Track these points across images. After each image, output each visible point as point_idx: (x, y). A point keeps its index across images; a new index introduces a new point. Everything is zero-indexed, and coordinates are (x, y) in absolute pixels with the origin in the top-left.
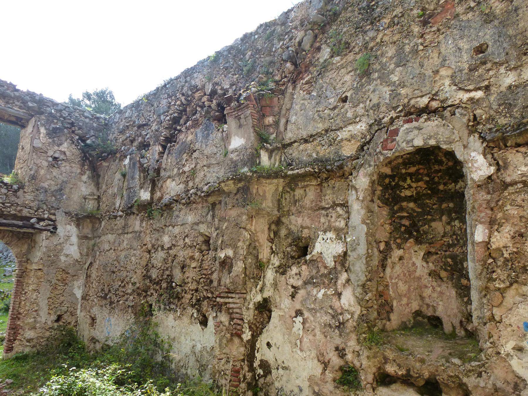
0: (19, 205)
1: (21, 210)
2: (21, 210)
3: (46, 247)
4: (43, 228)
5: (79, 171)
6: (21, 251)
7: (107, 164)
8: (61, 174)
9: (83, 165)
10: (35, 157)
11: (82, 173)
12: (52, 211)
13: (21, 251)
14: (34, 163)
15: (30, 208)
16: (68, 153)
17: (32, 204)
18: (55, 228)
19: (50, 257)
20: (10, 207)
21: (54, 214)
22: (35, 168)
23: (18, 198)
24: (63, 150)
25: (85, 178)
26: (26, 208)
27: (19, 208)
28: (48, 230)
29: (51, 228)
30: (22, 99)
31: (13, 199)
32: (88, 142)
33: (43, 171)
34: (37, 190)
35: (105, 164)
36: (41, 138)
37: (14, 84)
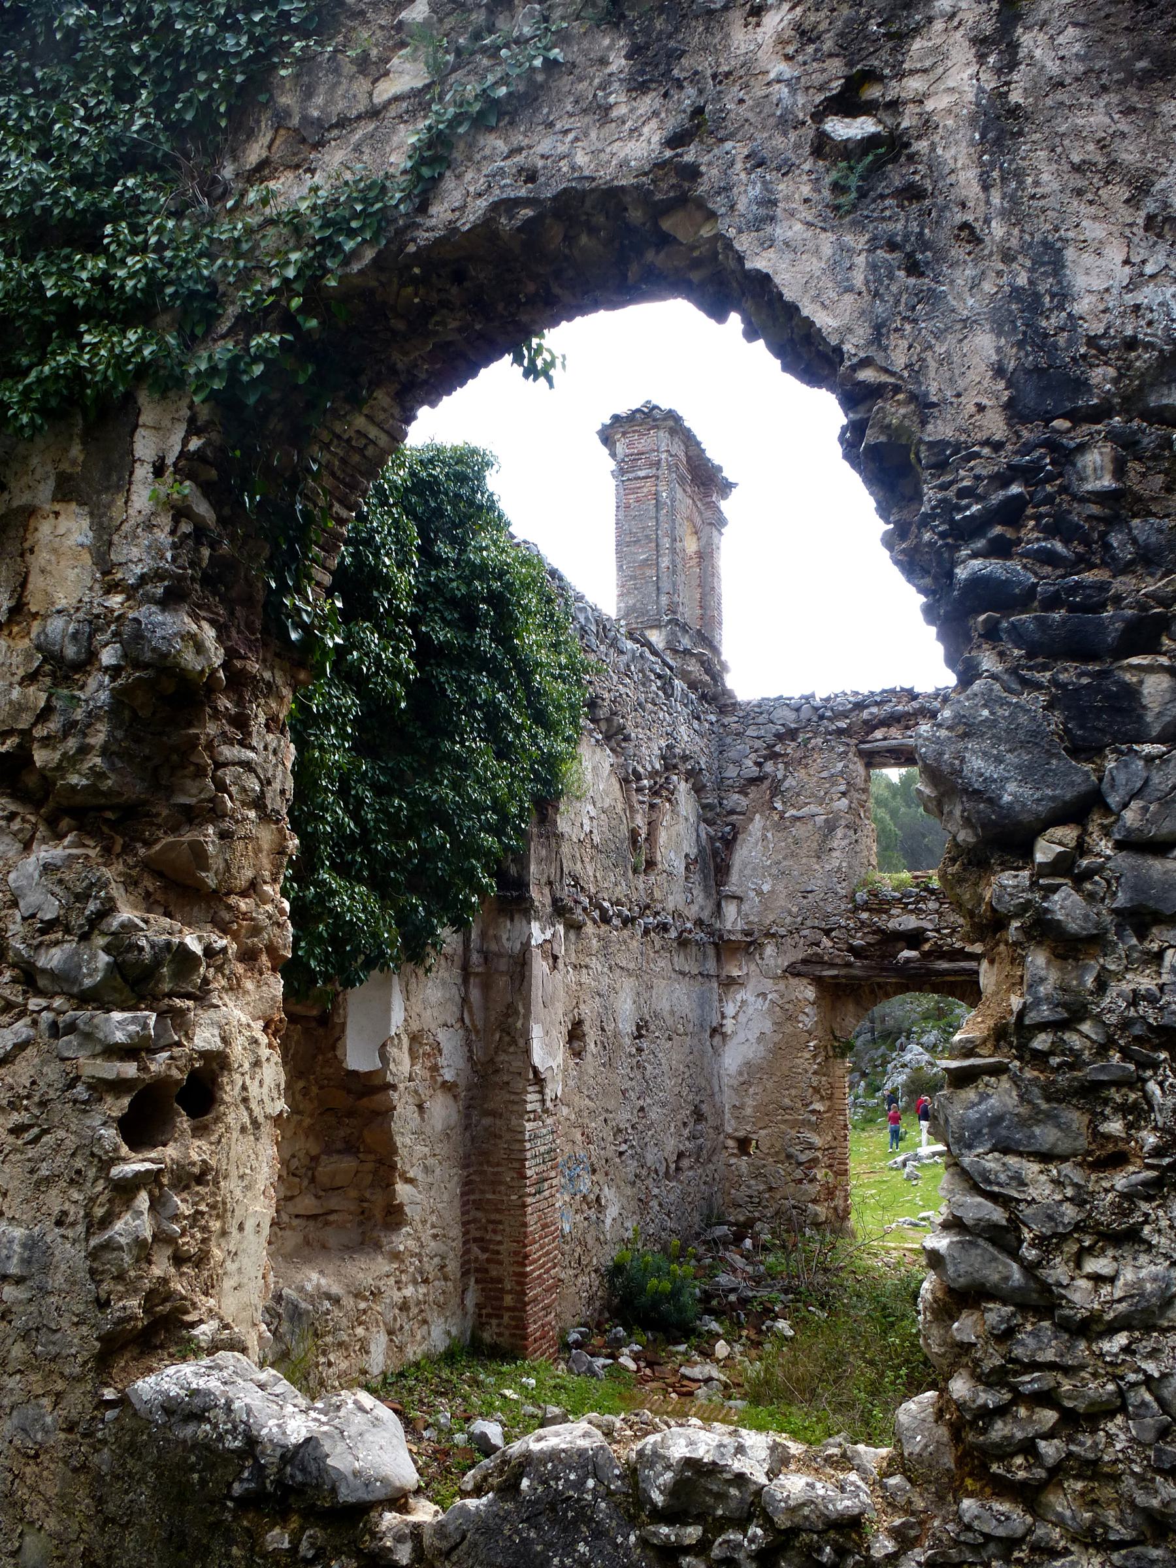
20: (951, 935)
30: (929, 711)
37: (907, 686)
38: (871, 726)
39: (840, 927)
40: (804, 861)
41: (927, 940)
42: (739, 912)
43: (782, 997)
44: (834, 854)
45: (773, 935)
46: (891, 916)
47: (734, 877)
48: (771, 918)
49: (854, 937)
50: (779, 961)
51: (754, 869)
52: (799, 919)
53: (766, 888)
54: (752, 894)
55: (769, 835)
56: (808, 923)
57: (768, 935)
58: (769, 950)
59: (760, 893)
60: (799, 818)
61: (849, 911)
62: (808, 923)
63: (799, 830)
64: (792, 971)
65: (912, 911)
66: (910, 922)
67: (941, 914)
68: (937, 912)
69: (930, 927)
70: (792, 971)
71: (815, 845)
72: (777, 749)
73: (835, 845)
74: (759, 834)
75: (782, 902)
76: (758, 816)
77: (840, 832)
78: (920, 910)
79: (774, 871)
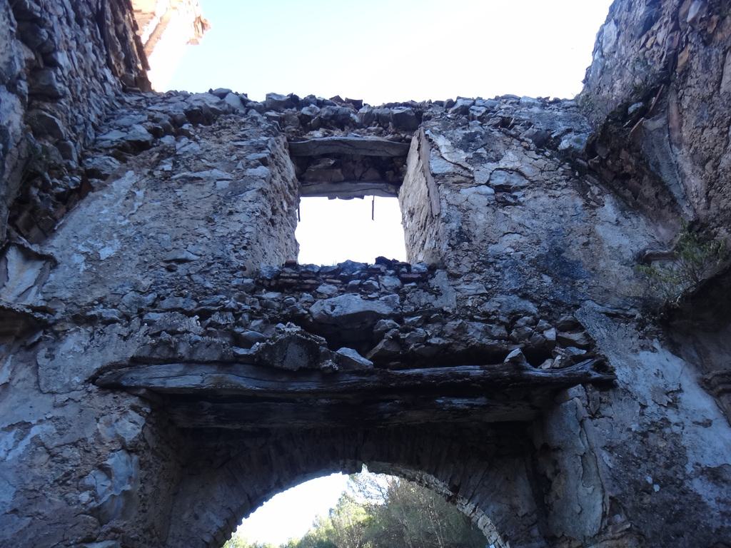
0: (446, 314)
1: (462, 329)
2: (462, 329)
3: (610, 448)
4: (559, 374)
5: (580, 202)
6: (513, 508)
7: (659, 123)
8: (535, 216)
9: (583, 191)
10: (447, 192)
11: (592, 205)
12: (566, 317)
13: (513, 508)
14: (449, 205)
15: (487, 318)
16: (526, 170)
17: (488, 307)
18: (602, 366)
19: (648, 490)
21: (576, 326)
22: (455, 213)
23: (438, 293)
24: (510, 166)
25: (609, 210)
26: (472, 319)
27: (452, 325)
28: (584, 380)
29: (586, 367)
31: (425, 298)
32: (564, 144)
33: (481, 216)
34: (487, 264)
35: (653, 124)
36: (445, 156)
38: (305, 124)
39: (224, 310)
40: (184, 223)
41: (381, 336)
42: (40, 281)
43: (60, 432)
44: (235, 217)
45: (92, 320)
46: (317, 295)
47: (57, 241)
48: (98, 293)
49: (246, 326)
50: (85, 360)
51: (98, 228)
52: (150, 298)
53: (106, 253)
54: (79, 259)
55: (140, 194)
56: (166, 304)
57: (82, 319)
58: (74, 341)
59: (92, 259)
60: (192, 180)
61: (245, 288)
62: (166, 304)
63: (188, 192)
64: (108, 382)
65: (354, 289)
66: (354, 304)
67: (403, 295)
68: (397, 290)
69: (385, 310)
70: (108, 382)
71: (207, 208)
72: (186, 127)
73: (239, 207)
74: (124, 192)
75: (130, 272)
76: (130, 173)
77: (249, 195)
78: (370, 288)
79: (130, 232)
